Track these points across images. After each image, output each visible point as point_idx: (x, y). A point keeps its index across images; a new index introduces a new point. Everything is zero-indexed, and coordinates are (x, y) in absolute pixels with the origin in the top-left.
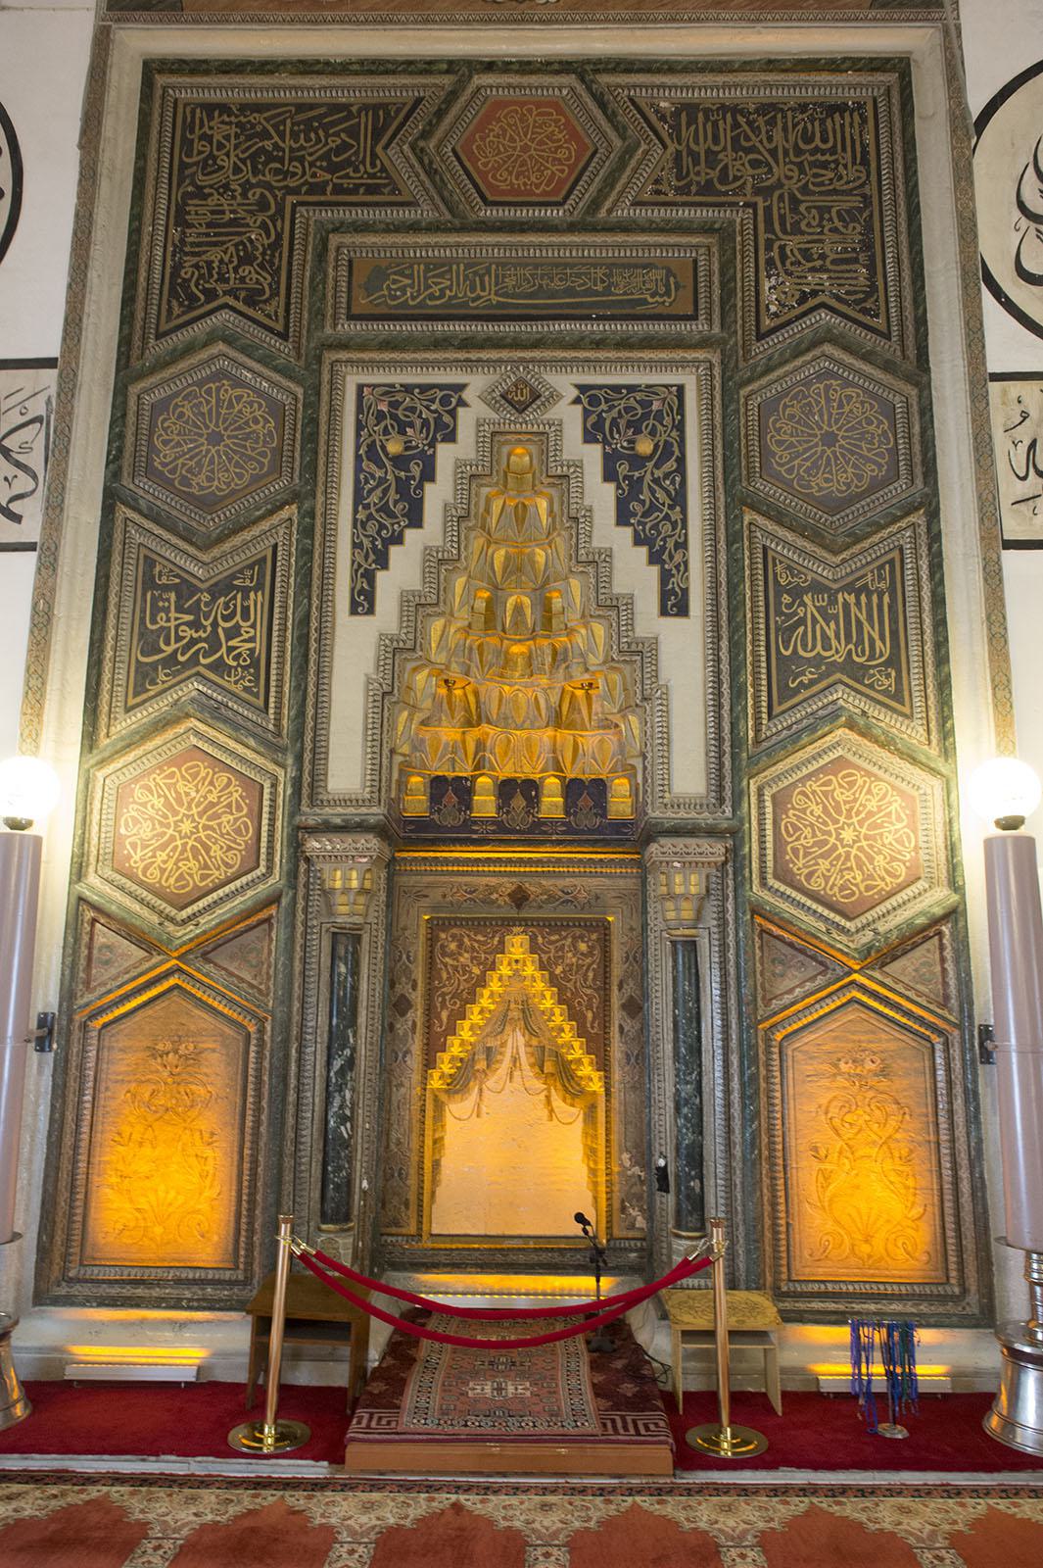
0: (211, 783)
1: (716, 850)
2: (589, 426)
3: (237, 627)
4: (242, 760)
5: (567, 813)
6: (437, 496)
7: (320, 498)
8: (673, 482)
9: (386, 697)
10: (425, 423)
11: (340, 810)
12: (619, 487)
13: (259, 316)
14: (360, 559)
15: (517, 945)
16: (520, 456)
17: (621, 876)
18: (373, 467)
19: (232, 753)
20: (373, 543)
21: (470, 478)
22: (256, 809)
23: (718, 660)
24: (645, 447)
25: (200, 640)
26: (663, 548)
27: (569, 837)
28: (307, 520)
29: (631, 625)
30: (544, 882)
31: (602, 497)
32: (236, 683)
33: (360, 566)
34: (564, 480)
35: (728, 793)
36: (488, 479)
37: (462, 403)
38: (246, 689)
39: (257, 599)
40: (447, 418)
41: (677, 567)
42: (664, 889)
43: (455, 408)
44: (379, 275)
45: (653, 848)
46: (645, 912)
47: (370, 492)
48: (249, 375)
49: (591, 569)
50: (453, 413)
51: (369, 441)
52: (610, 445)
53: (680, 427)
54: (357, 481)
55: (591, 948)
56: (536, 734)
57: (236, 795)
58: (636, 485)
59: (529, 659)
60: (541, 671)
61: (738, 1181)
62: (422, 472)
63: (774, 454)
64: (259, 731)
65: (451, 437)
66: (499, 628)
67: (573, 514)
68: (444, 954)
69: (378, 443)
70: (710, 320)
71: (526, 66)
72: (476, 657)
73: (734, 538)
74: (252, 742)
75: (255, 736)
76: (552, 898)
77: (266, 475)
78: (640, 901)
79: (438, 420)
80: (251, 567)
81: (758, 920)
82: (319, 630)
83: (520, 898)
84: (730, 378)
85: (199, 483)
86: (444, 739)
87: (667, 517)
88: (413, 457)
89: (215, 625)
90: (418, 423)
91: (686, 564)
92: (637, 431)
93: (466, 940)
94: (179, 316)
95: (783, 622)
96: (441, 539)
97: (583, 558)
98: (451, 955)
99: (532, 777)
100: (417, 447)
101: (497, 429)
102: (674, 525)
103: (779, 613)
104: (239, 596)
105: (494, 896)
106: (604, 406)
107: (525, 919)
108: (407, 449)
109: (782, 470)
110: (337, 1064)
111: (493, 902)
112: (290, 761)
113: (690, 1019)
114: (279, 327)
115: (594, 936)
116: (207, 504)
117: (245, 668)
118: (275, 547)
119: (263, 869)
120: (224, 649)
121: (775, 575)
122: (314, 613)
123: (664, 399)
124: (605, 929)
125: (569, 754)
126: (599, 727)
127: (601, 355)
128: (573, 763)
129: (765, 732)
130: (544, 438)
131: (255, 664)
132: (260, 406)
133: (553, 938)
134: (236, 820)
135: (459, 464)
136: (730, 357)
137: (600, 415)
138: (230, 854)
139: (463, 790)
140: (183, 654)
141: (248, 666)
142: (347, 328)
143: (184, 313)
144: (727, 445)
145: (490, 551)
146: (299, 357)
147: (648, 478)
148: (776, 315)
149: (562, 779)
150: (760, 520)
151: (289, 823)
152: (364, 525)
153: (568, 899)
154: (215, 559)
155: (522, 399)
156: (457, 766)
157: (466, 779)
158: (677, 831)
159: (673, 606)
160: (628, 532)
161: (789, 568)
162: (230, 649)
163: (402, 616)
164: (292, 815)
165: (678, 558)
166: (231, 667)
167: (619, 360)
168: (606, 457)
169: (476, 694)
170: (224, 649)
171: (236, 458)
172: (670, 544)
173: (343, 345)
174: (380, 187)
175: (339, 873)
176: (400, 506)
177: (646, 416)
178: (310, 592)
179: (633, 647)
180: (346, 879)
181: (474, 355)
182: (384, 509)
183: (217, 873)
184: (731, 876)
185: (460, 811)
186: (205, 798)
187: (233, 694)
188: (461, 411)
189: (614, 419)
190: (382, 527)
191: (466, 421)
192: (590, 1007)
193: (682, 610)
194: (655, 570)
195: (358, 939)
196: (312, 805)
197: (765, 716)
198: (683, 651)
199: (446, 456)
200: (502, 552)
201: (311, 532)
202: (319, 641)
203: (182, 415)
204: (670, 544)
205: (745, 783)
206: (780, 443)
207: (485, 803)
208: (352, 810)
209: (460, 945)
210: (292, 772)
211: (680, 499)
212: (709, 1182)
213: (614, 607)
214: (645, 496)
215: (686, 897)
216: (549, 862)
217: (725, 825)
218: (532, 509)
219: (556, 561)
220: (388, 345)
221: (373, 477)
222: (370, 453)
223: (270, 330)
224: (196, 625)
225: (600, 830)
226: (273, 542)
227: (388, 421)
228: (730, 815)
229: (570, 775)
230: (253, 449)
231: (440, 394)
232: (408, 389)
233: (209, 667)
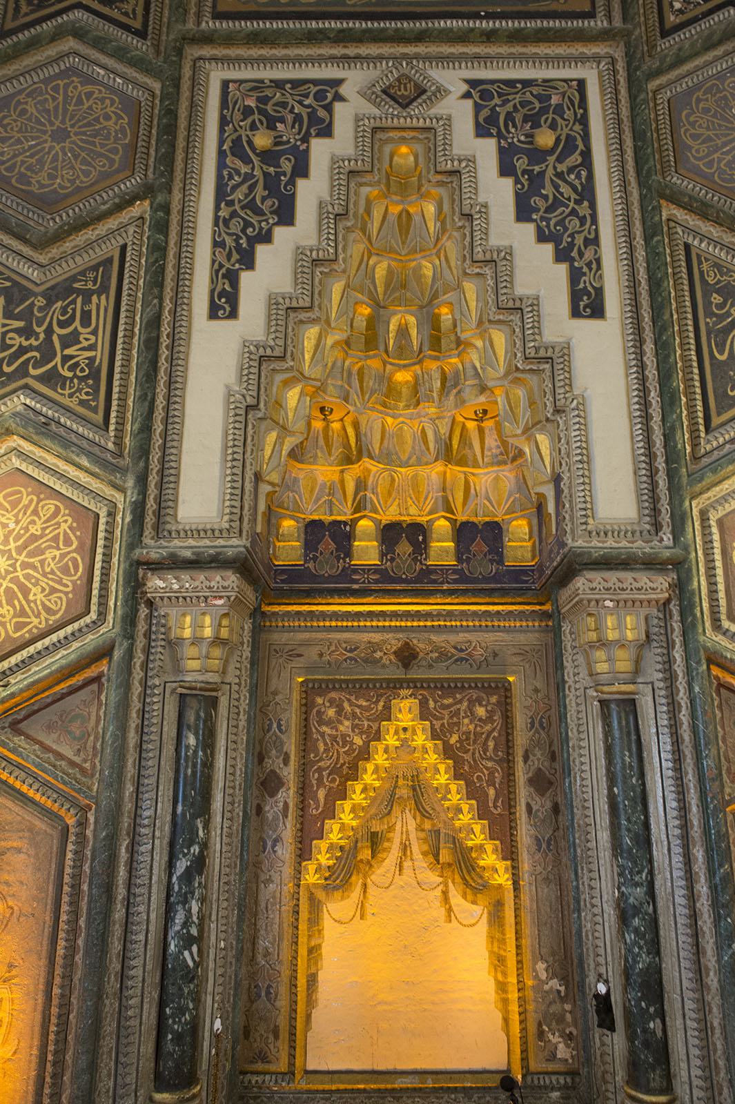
0: (35, 512)
1: (659, 585)
2: (481, 120)
3: (76, 333)
4: (74, 484)
5: (459, 559)
6: (310, 194)
7: (177, 196)
8: (578, 176)
9: (250, 412)
10: (298, 118)
11: (191, 542)
12: (517, 182)
13: (115, 14)
14: (221, 258)
15: (405, 711)
16: (405, 156)
17: (521, 630)
18: (238, 163)
19: (61, 476)
20: (237, 241)
21: (349, 175)
22: (89, 542)
23: (642, 367)
24: (545, 139)
25: (31, 348)
26: (571, 245)
27: (462, 587)
28: (161, 214)
29: (538, 328)
30: (434, 638)
31: (498, 193)
32: (71, 396)
33: (221, 266)
34: (455, 176)
35: (665, 518)
36: (368, 178)
37: (339, 98)
38: (82, 403)
39: (101, 305)
40: (322, 113)
41: (589, 265)
42: (593, 636)
43: (331, 103)
45: (580, 583)
46: (560, 667)
47: (234, 188)
48: (102, 72)
49: (488, 271)
50: (329, 108)
51: (234, 136)
52: (506, 139)
53: (584, 121)
54: (219, 177)
55: (491, 714)
56: (423, 471)
57: (64, 526)
58: (536, 181)
59: (416, 386)
60: (429, 399)
61: (716, 1024)
62: (294, 167)
63: (690, 148)
64: (96, 450)
65: (326, 131)
66: (382, 348)
67: (466, 210)
68: (321, 722)
69: (244, 138)
70: (609, 18)
72: (356, 383)
73: (651, 232)
74: (85, 462)
75: (89, 455)
76: (444, 656)
77: (117, 171)
78: (551, 660)
79: (312, 116)
80: (95, 268)
81: (715, 671)
82: (172, 336)
83: (407, 656)
84: (637, 68)
85: (40, 182)
86: (320, 479)
87: (574, 212)
88: (283, 152)
89: (49, 332)
90: (290, 118)
91: (598, 261)
92: (536, 125)
93: (346, 705)
94: (26, 14)
95: (715, 324)
96: (315, 236)
97: (480, 257)
98: (329, 723)
99: (419, 520)
100: (288, 142)
101: (378, 124)
102: (582, 220)
103: (709, 314)
104: (79, 300)
105: (378, 654)
106: (497, 101)
107: (414, 681)
108: (276, 144)
109: (701, 164)
110: (182, 865)
111: (377, 662)
112: (130, 483)
113: (630, 803)
114: (137, 25)
115: (494, 699)
116: (47, 203)
117: (81, 379)
118: (124, 248)
119: (93, 615)
120: (58, 359)
121: (701, 273)
122: (166, 317)
123: (564, 94)
124: (505, 691)
125: (460, 496)
126: (492, 464)
127: (493, 50)
128: (464, 504)
129: (705, 447)
130: (431, 136)
131: (95, 374)
132: (113, 102)
133: (446, 702)
134: (63, 556)
135: (335, 160)
136: (636, 47)
137: (493, 110)
138: (53, 597)
139: (342, 535)
140: (9, 365)
141: (87, 377)
143: (32, 12)
144: (638, 136)
145: (371, 262)
146: (158, 53)
147: (550, 172)
148: (681, 11)
149: (453, 522)
150: (680, 214)
151: (127, 557)
152: (226, 222)
153: (462, 657)
154: (53, 261)
155: (405, 94)
156: (335, 509)
157: (345, 523)
158: (607, 563)
159: (586, 307)
160: (530, 228)
161: (716, 265)
162: (66, 358)
163: (270, 321)
164: (131, 547)
165: (589, 254)
166: (66, 378)
167: (511, 56)
168: (502, 151)
169: (356, 425)
170: (58, 359)
171: (83, 154)
172: (579, 240)
173: (207, 39)
175: (188, 619)
176: (269, 202)
177: (543, 110)
178: (161, 292)
179: (542, 353)
180: (197, 626)
181: (351, 51)
182: (251, 206)
183: (36, 621)
184: (676, 617)
185: (338, 558)
186: (27, 529)
187: (67, 409)
188: (338, 107)
189: (508, 114)
190: (247, 224)
191: (343, 116)
192: (491, 782)
193: (597, 311)
194: (563, 268)
195: (214, 702)
196: (158, 535)
197: (702, 428)
198: (600, 358)
199: (320, 151)
200: (385, 265)
201: (165, 232)
202: (171, 347)
203: (24, 112)
204: (579, 240)
205: (687, 503)
206: (695, 137)
207: (367, 550)
208: (207, 542)
209: (340, 710)
210: (132, 495)
211: (587, 193)
212: (675, 1023)
213: (518, 312)
214: (548, 190)
215: (621, 644)
216: (439, 615)
217: (667, 554)
218: (417, 218)
219: (446, 271)
220: (256, 39)
221: (238, 173)
222: (235, 148)
223: (127, 28)
224: (27, 332)
225: (496, 578)
226: (122, 242)
227: (256, 116)
228: (671, 543)
229: (462, 518)
230: (102, 146)
231: (314, 89)
232: (279, 84)
233: (39, 378)
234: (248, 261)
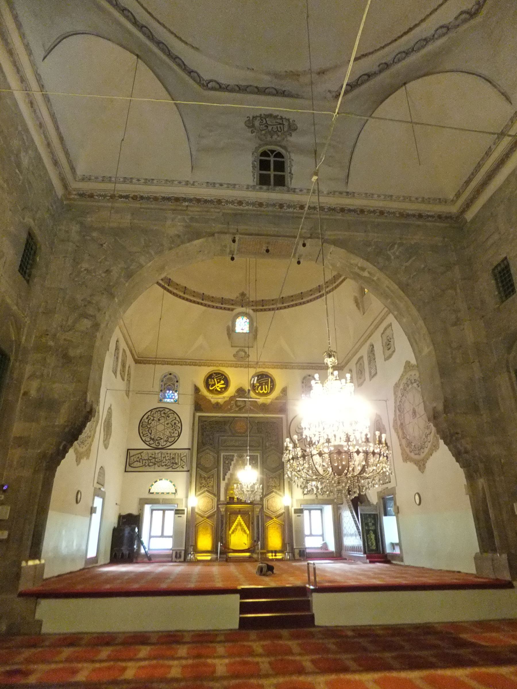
6: (231, 467)
39: (212, 479)
71: (241, 417)
116: (207, 468)
142: (222, 448)
174: (225, 431)
199: (232, 463)
234: (226, 475)
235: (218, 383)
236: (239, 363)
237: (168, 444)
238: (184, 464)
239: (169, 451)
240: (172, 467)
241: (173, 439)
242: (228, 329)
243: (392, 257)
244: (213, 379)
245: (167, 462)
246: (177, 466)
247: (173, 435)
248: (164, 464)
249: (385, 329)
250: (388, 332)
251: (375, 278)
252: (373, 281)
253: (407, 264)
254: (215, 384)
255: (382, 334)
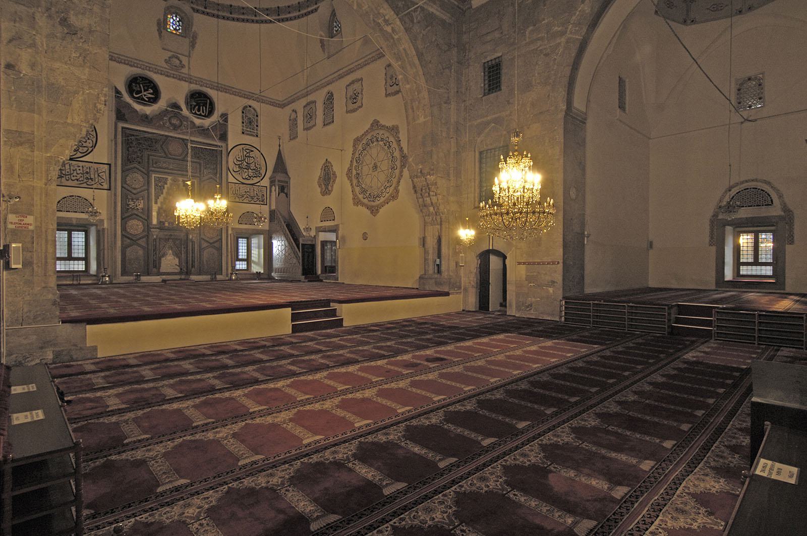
6: (165, 191)
44: (156, 163)
85: (133, 186)
116: (135, 189)
135: (168, 187)
142: (153, 169)
222: (156, 185)
235: (144, 91)
236: (173, 72)
237: (79, 155)
238: (103, 181)
239: (81, 164)
240: (86, 182)
241: (85, 149)
242: (159, 24)
243: (415, 21)
244: (139, 84)
245: (79, 176)
246: (93, 183)
247: (85, 145)
248: (75, 178)
249: (353, 83)
250: (357, 86)
251: (396, 37)
252: (393, 38)
253: (424, 33)
254: (141, 92)
255: (348, 85)
